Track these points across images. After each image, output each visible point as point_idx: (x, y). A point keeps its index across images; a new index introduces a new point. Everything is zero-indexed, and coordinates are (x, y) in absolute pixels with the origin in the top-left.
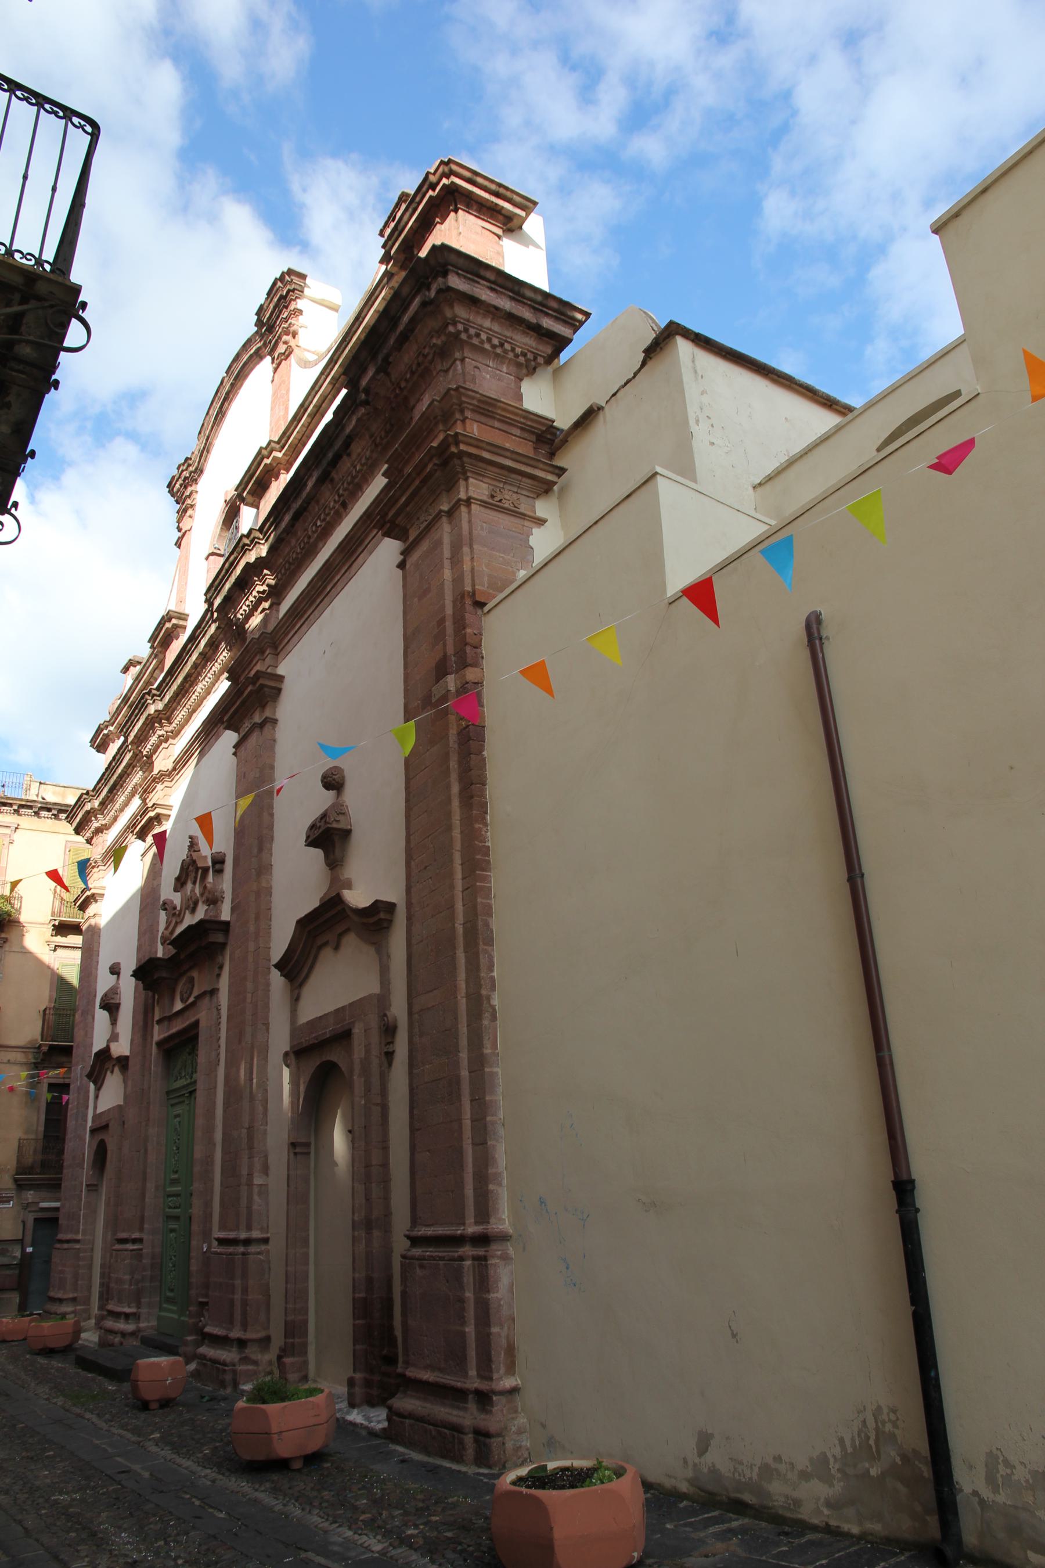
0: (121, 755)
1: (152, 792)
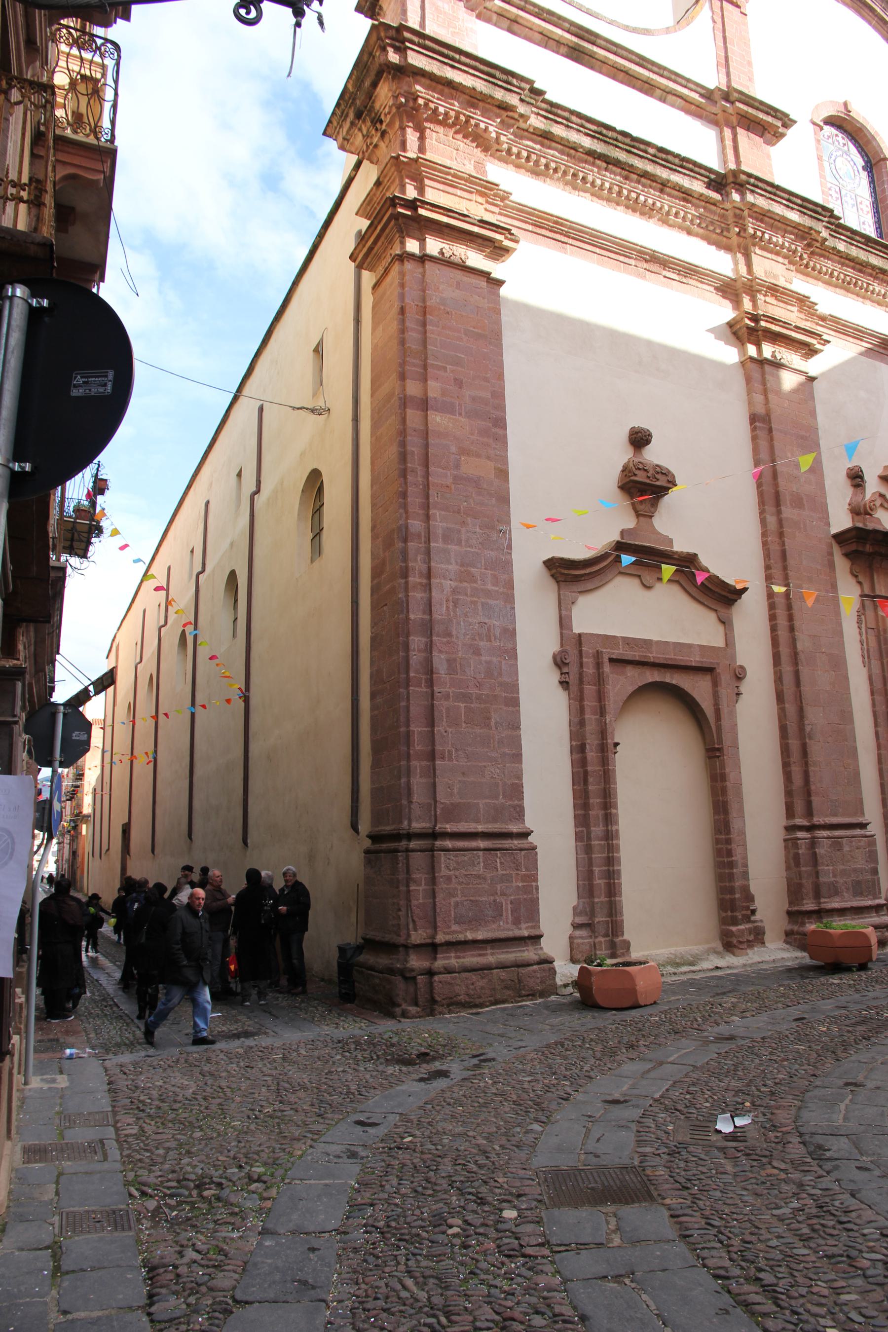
0: (681, 167)
1: (776, 299)
